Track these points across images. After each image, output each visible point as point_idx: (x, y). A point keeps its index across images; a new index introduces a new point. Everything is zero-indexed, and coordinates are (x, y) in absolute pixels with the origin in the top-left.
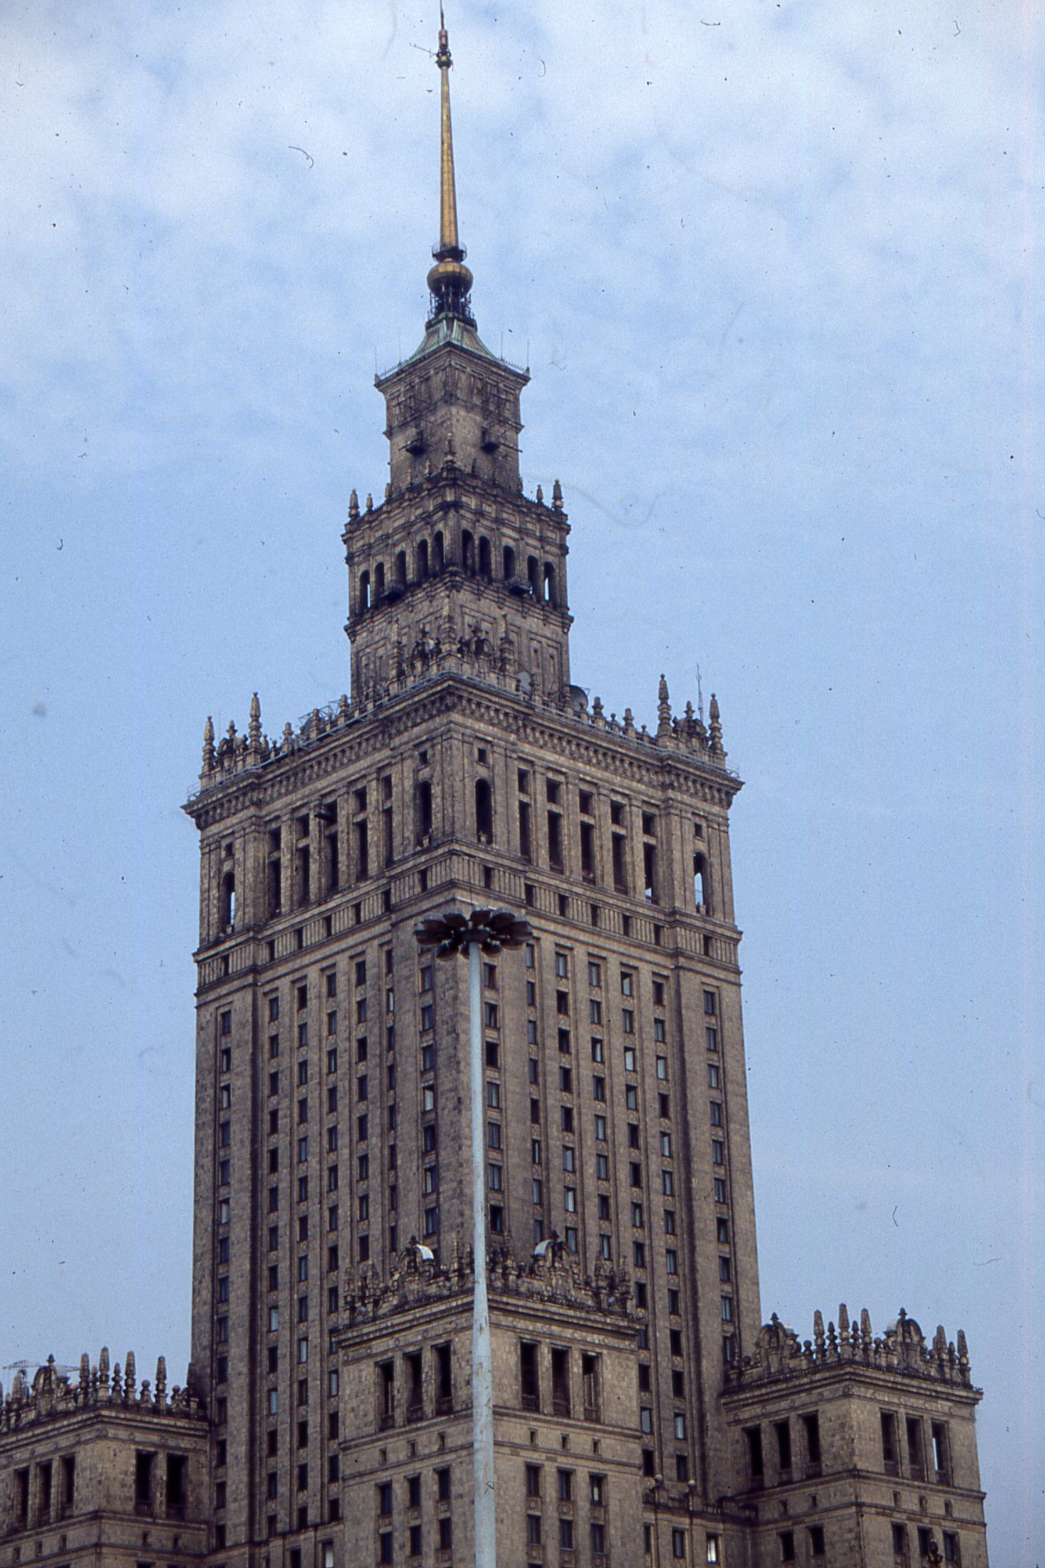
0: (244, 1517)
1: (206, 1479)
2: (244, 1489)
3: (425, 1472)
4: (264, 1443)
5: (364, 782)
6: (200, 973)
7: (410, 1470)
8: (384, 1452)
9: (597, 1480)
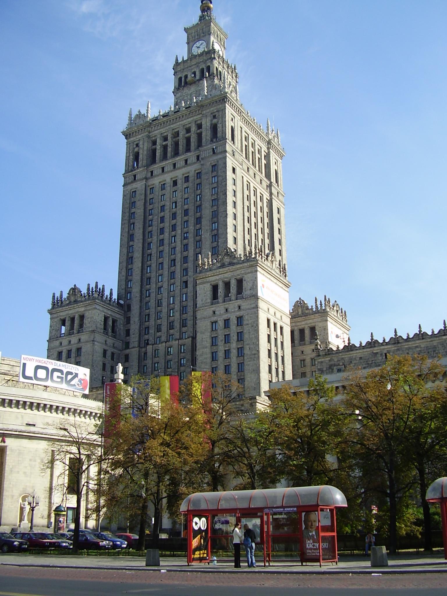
0: (137, 339)
1: (122, 328)
2: (137, 331)
3: (232, 317)
4: (144, 318)
5: (190, 125)
6: (125, 180)
7: (226, 317)
8: (214, 312)
9: (281, 328)
